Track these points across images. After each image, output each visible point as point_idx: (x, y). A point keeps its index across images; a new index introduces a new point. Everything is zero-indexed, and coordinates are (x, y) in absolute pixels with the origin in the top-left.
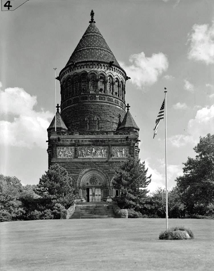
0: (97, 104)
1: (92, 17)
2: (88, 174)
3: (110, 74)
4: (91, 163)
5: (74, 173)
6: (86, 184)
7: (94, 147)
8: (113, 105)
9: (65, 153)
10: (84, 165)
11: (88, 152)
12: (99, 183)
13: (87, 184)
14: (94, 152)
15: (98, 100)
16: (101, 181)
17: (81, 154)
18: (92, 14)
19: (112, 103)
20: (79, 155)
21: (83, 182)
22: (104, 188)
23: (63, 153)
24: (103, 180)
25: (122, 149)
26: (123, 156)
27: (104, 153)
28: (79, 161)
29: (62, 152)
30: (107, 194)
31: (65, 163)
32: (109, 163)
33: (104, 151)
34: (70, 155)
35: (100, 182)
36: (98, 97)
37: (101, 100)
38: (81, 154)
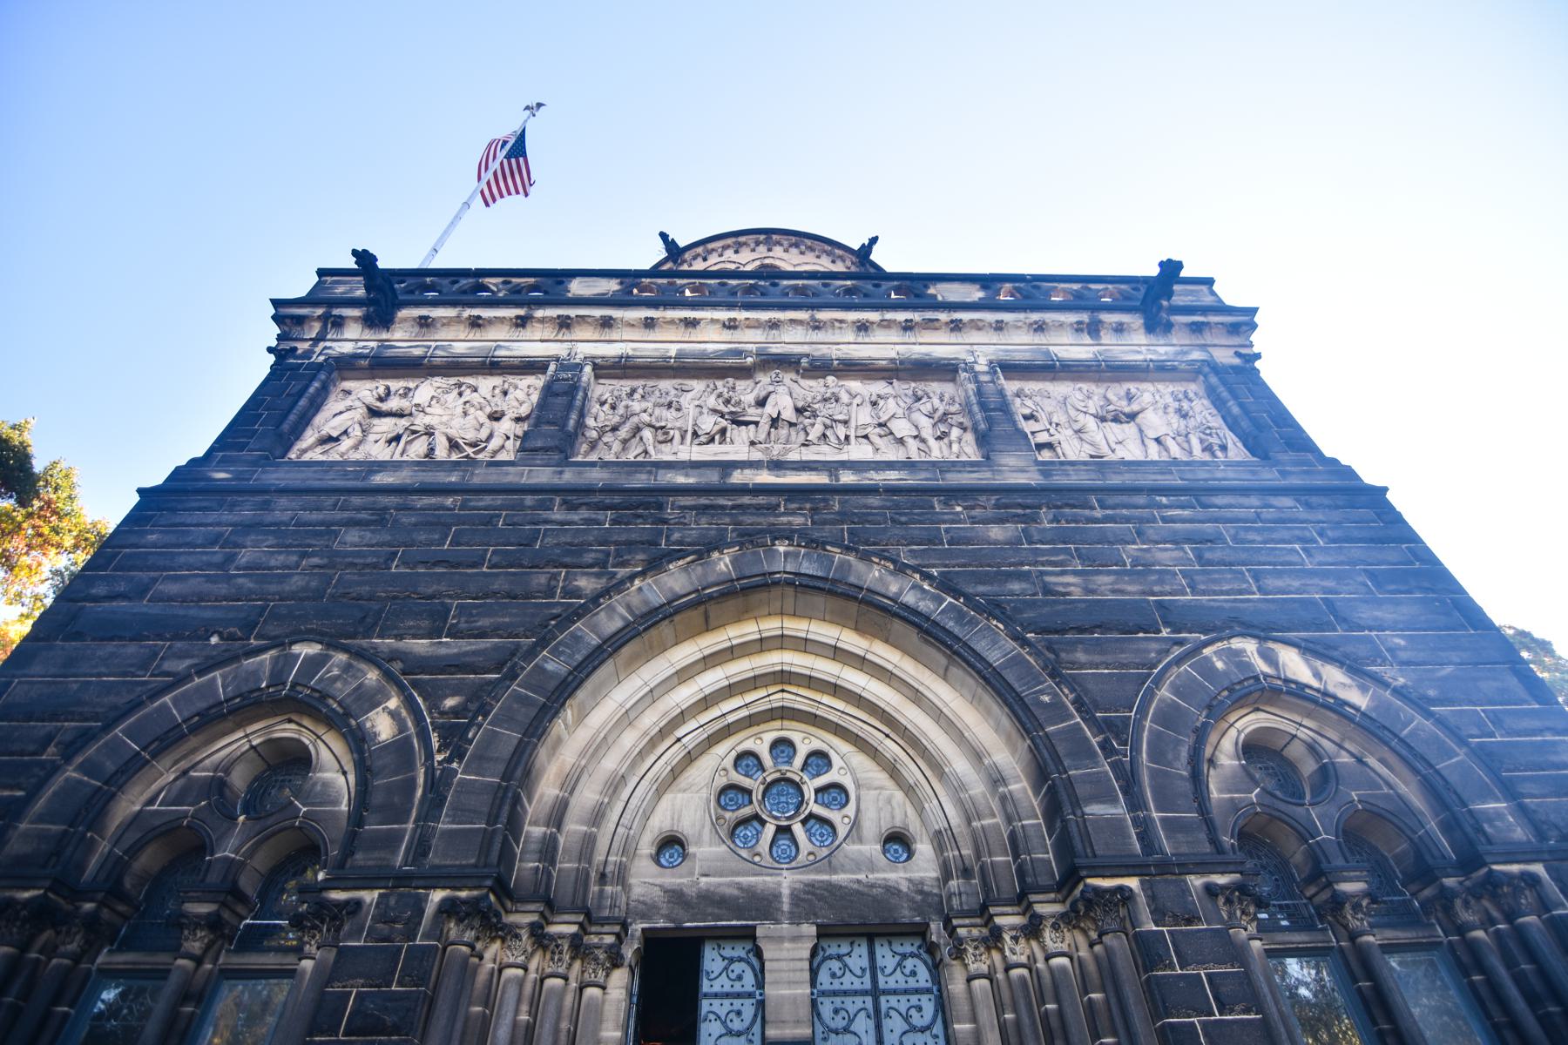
2: (684, 675)
4: (746, 500)
7: (788, 377)
12: (873, 825)
14: (788, 414)
16: (909, 790)
21: (587, 795)
22: (1008, 920)
23: (385, 426)
24: (960, 765)
28: (568, 477)
35: (901, 812)
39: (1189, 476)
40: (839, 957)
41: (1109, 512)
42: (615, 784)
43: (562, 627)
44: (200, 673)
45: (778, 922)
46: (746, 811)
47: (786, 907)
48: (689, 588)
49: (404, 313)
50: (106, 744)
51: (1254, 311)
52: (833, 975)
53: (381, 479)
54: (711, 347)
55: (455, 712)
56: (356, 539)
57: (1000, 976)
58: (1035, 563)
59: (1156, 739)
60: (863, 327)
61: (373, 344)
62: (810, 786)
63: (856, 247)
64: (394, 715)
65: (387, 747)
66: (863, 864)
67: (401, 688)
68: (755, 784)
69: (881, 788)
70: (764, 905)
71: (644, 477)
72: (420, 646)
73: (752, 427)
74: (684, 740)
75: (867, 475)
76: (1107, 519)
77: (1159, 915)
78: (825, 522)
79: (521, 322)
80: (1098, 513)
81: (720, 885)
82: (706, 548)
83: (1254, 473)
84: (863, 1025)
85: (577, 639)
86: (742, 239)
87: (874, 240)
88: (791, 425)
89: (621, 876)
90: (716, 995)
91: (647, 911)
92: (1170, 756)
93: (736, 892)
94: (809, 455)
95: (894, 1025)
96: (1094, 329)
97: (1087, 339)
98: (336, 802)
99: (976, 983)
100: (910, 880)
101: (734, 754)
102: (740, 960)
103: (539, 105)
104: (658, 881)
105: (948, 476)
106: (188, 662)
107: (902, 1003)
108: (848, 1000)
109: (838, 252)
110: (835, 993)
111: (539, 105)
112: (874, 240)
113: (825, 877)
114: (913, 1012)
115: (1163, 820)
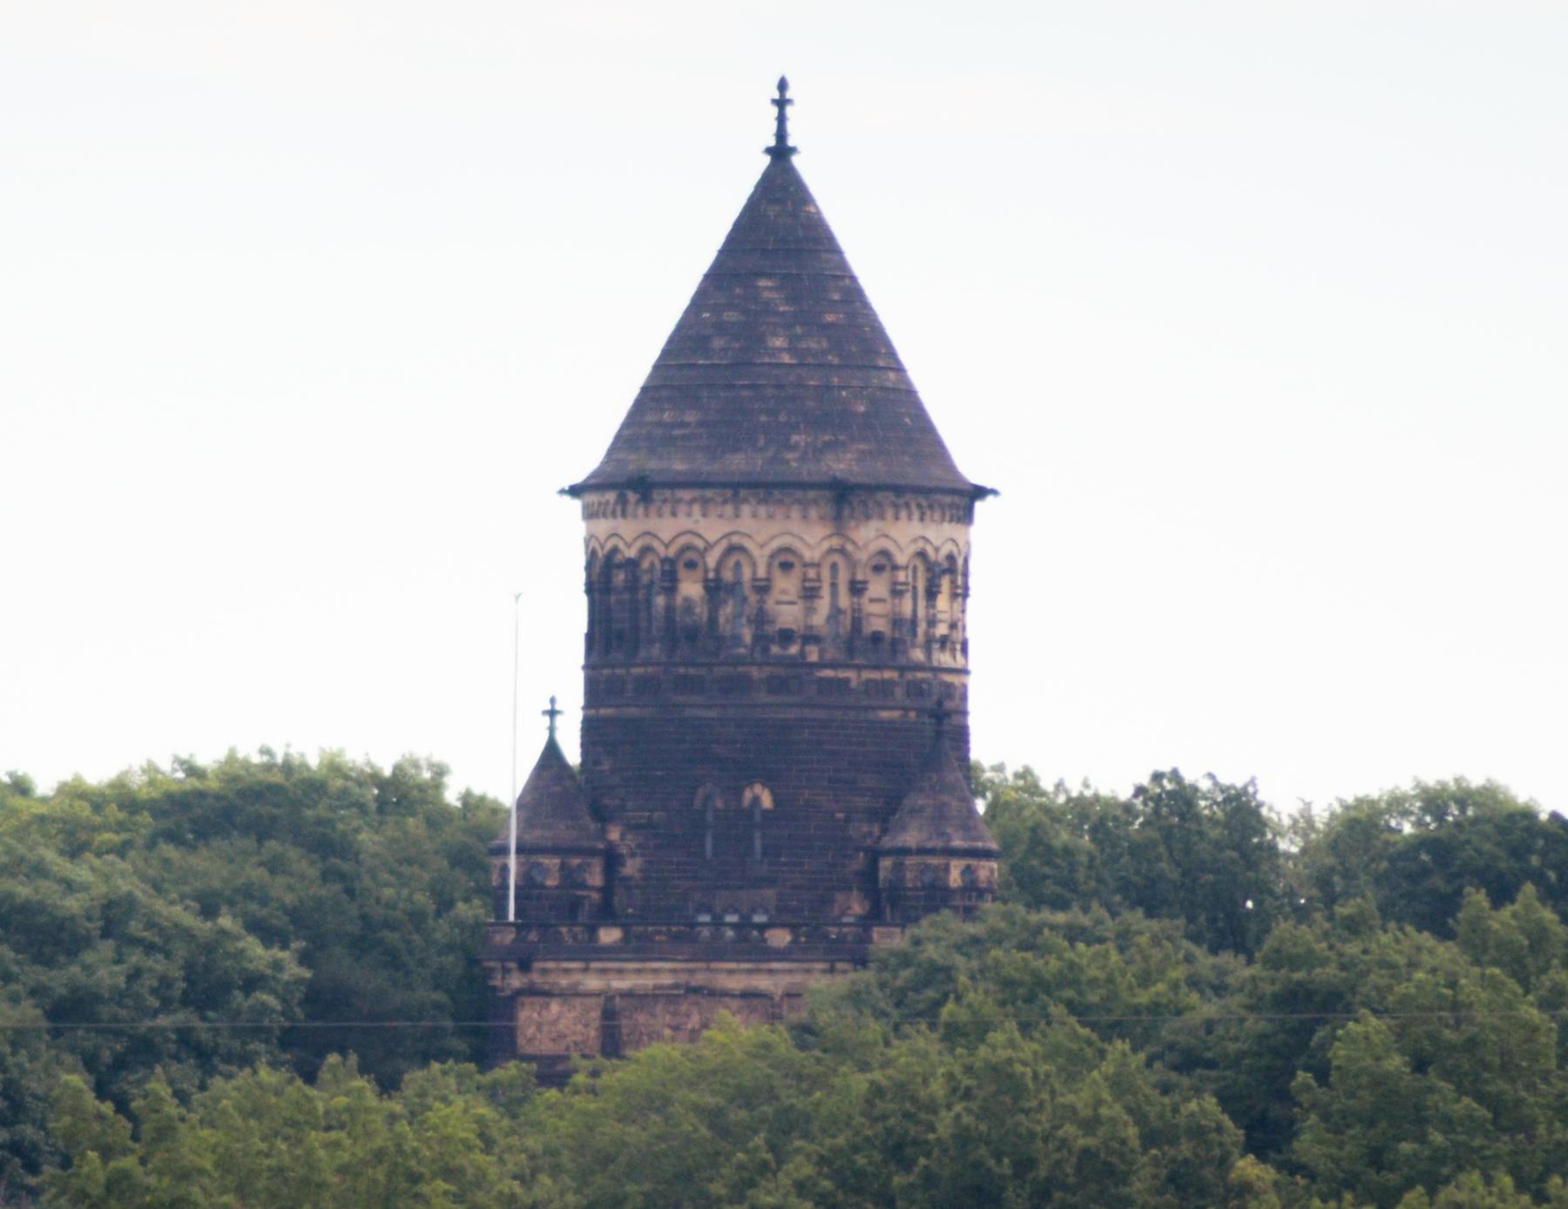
1: (781, 119)
8: (852, 715)
60: (731, 972)
86: (709, 493)
109: (811, 494)
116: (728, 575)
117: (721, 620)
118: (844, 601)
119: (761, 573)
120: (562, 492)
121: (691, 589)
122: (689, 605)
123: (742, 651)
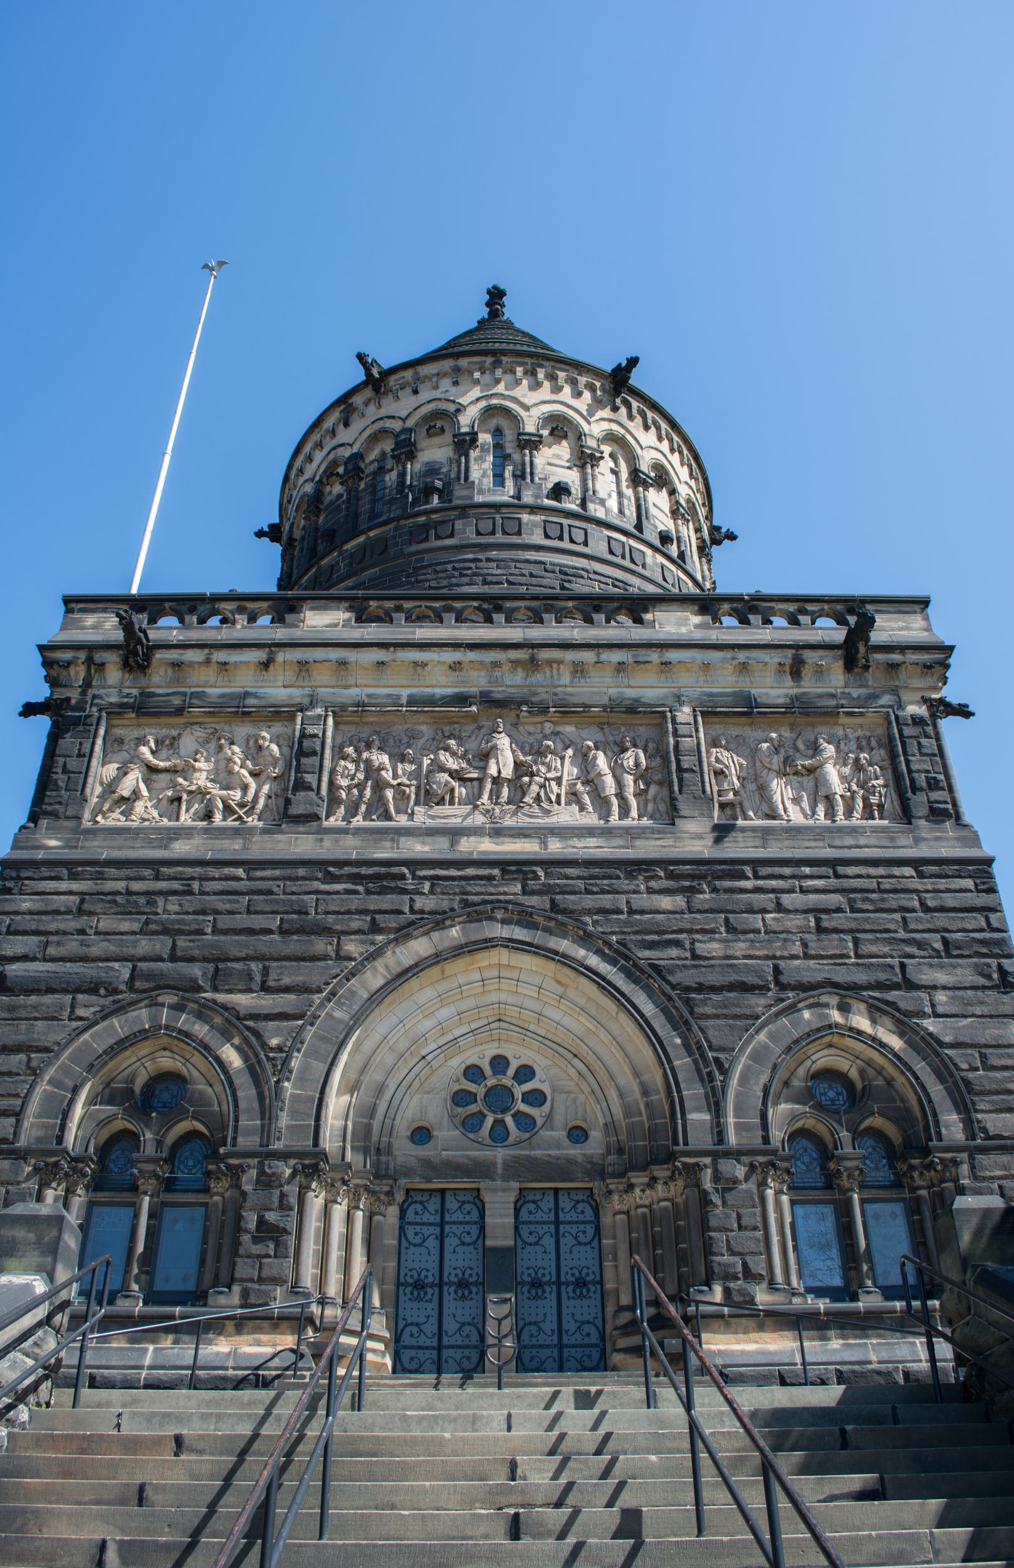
0: (528, 561)
3: (614, 427)
4: (470, 871)
5: (250, 976)
6: (403, 1129)
9: (175, 785)
10: (383, 891)
11: (442, 769)
13: (421, 1134)
14: (508, 772)
15: (534, 537)
17: (361, 786)
18: (496, 296)
19: (639, 569)
20: (334, 801)
23: (164, 778)
25: (816, 749)
26: (831, 813)
27: (620, 784)
29: (152, 770)
30: (683, 1258)
31: (157, 878)
32: (693, 877)
33: (617, 771)
34: (237, 795)
36: (535, 525)
37: (561, 538)
38: (361, 786)
39: (838, 843)
40: (534, 1202)
41: (760, 883)
42: (380, 1090)
43: (340, 985)
44: (104, 1018)
45: (493, 1180)
46: (473, 1108)
47: (499, 1171)
48: (431, 951)
49: (158, 655)
50: (59, 1067)
51: (950, 649)
52: (530, 1212)
53: (181, 848)
54: (439, 691)
55: (279, 1049)
56: (176, 908)
57: (632, 1213)
58: (690, 931)
59: (747, 1069)
61: (135, 692)
62: (519, 1091)
63: (608, 368)
64: (238, 1049)
65: (239, 1071)
66: (552, 1142)
67: (241, 1033)
68: (480, 1090)
69: (570, 1092)
70: (483, 1170)
71: (388, 844)
72: (243, 1001)
73: (476, 783)
74: (429, 1058)
75: (571, 843)
76: (758, 890)
77: (717, 1177)
78: (533, 893)
79: (266, 665)
80: (748, 884)
81: (456, 1156)
82: (439, 920)
83: (892, 839)
84: (549, 1242)
85: (353, 993)
86: (463, 362)
87: (633, 362)
88: (509, 780)
89: (389, 1150)
90: (454, 1223)
91: (407, 1172)
92: (752, 1082)
93: (466, 1161)
94: (521, 820)
95: (567, 1242)
96: (796, 671)
97: (788, 681)
98: (210, 1105)
99: (618, 1217)
100: (584, 1155)
101: (463, 1066)
102: (469, 1202)
103: (221, 264)
104: (414, 1153)
105: (638, 843)
106: (92, 1009)
107: (574, 1229)
108: (539, 1227)
110: (530, 1223)
111: (221, 264)
112: (633, 362)
113: (527, 1153)
114: (580, 1234)
115: (736, 1124)
116: (485, 438)
117: (475, 474)
118: (629, 492)
119: (530, 428)
120: (260, 534)
121: (435, 452)
122: (432, 470)
123: (505, 499)
